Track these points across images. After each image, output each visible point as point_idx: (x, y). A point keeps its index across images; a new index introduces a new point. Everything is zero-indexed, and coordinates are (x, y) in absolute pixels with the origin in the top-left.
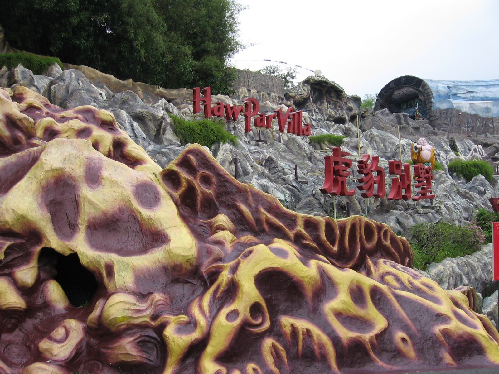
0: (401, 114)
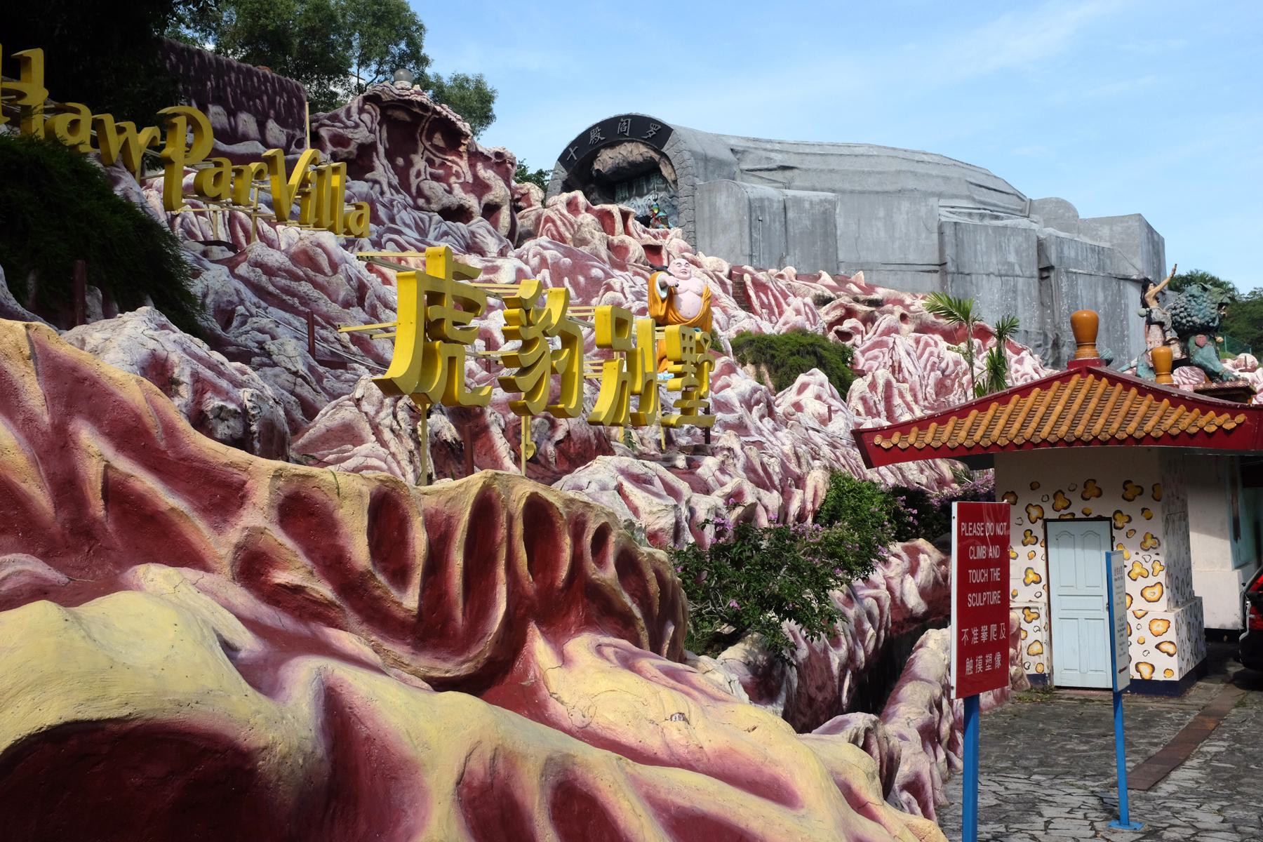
0: (614, 209)
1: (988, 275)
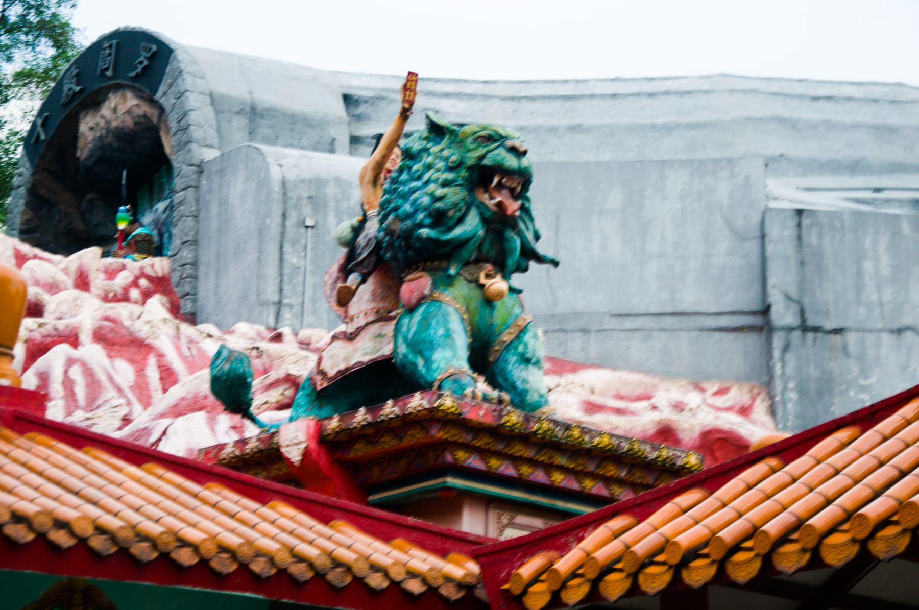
1: (899, 331)
